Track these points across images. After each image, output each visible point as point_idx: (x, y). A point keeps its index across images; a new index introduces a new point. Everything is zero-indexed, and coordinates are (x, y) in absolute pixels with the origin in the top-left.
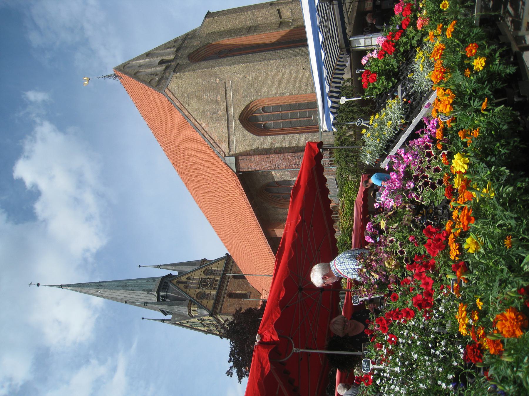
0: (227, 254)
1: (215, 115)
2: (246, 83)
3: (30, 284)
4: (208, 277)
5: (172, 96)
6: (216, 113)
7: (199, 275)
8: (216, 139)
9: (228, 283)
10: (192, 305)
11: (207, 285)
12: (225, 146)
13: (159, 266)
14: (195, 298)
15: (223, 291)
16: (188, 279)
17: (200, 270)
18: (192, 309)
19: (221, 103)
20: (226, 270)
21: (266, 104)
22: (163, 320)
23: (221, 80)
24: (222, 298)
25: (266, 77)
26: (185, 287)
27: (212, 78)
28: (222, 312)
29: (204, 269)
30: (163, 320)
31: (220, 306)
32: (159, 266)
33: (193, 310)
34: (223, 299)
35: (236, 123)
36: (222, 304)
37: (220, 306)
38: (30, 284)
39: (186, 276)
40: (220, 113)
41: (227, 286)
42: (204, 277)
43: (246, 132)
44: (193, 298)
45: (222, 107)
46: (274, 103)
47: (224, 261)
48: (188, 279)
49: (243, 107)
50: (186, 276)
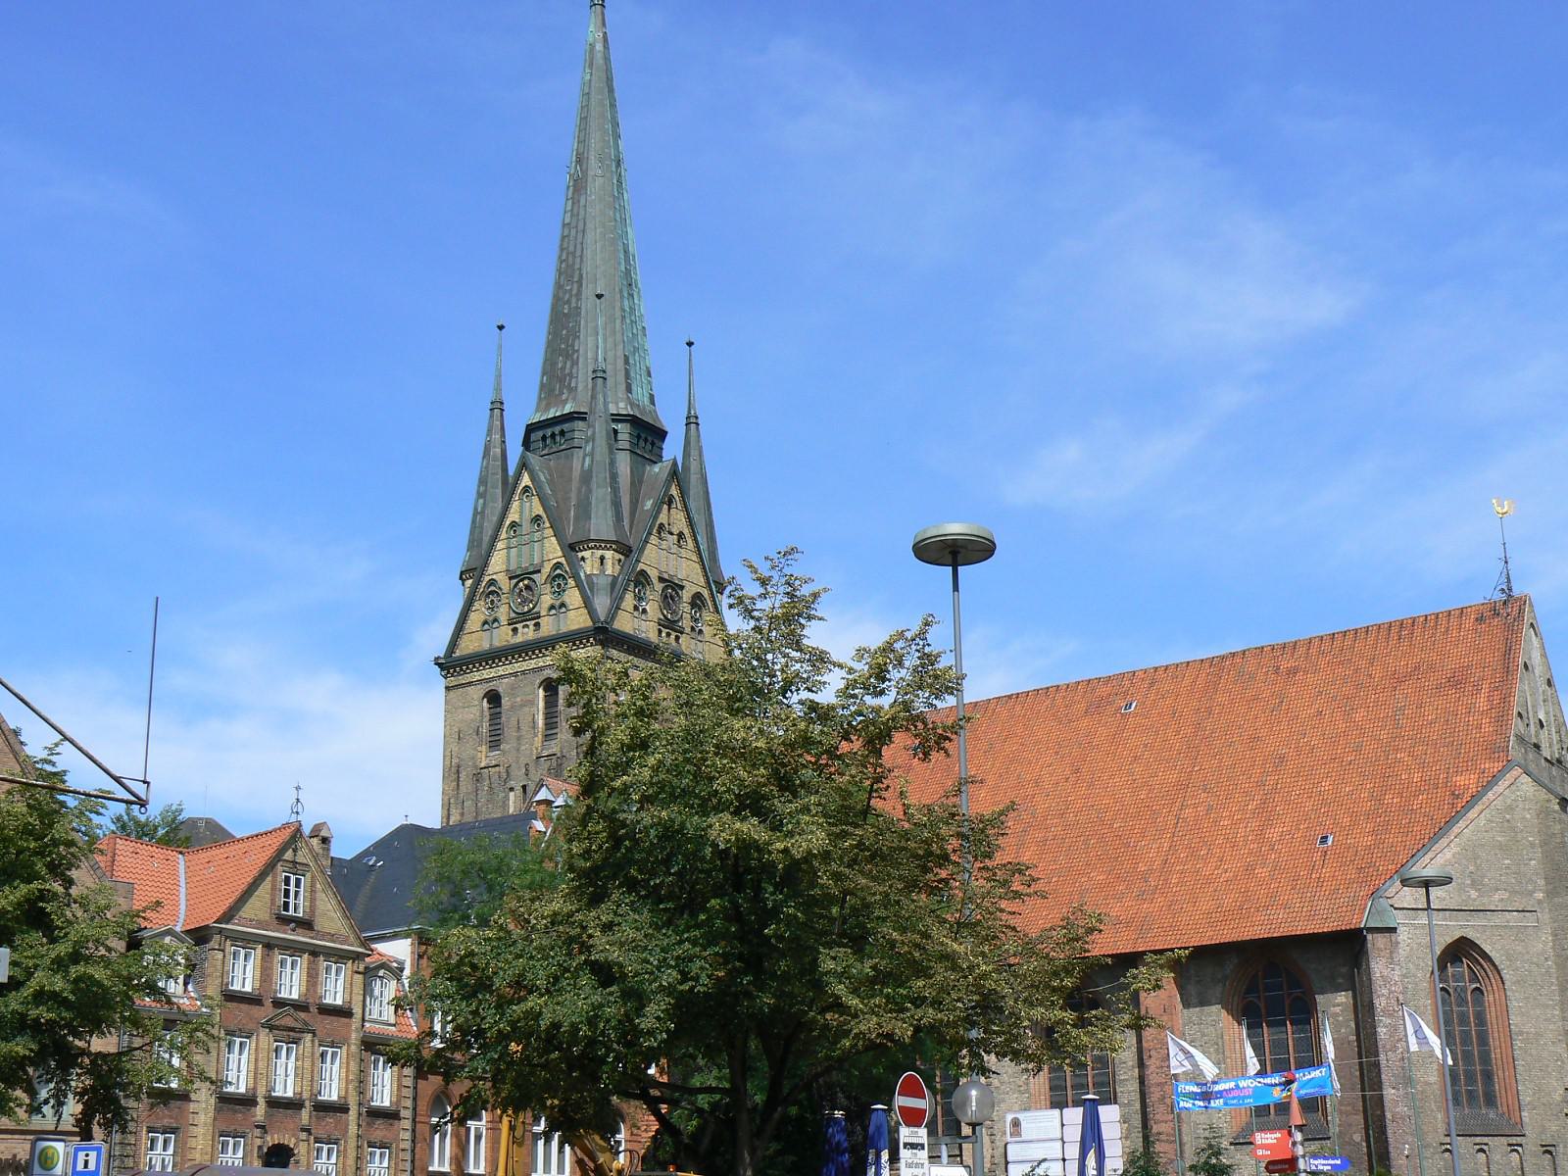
1: (1469, 882)
2: (1535, 960)
4: (687, 608)
5: (1507, 783)
6: (1473, 884)
10: (618, 556)
11: (668, 606)
13: (692, 421)
16: (681, 535)
18: (609, 554)
19: (1496, 900)
21: (1489, 998)
22: (498, 406)
23: (1540, 902)
25: (1548, 1006)
27: (1543, 882)
29: (706, 593)
30: (498, 406)
32: (692, 421)
33: (602, 558)
39: (686, 531)
40: (1474, 894)
42: (686, 595)
44: (638, 561)
45: (1485, 900)
46: (1491, 1015)
49: (1487, 948)
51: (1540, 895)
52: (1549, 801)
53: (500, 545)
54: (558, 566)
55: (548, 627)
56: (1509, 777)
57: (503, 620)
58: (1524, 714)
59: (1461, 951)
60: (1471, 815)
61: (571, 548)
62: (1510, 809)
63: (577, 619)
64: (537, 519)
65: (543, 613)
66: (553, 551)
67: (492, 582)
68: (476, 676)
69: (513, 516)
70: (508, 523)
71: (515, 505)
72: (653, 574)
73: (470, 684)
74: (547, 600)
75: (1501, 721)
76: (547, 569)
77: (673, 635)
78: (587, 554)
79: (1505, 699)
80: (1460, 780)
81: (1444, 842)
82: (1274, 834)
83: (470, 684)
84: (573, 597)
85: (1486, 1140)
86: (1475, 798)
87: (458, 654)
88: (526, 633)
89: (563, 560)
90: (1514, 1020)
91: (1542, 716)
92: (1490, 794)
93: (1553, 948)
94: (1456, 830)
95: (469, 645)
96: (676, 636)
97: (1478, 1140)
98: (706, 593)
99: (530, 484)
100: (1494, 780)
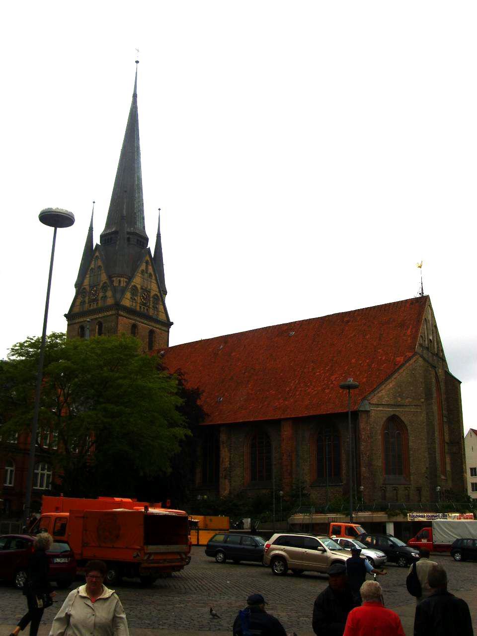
0: (172, 324)
3: (138, 51)
5: (414, 360)
7: (154, 287)
8: (380, 395)
9: (145, 324)
12: (375, 401)
14: (133, 284)
15: (138, 319)
17: (157, 290)
18: (122, 279)
20: (157, 321)
23: (422, 402)
24: (132, 317)
26: (143, 271)
28: (119, 317)
29: (159, 294)
31: (125, 314)
34: (131, 319)
35: (391, 411)
36: (126, 317)
37: (125, 314)
38: (138, 51)
39: (152, 273)
40: (399, 399)
41: (142, 323)
43: (384, 419)
47: (165, 319)
48: (150, 275)
50: (152, 273)
51: (423, 400)
52: (428, 367)
53: (88, 276)
54: (105, 283)
55: (100, 304)
56: (415, 358)
57: (87, 301)
58: (424, 337)
59: (394, 420)
60: (401, 371)
61: (110, 277)
62: (414, 369)
63: (110, 301)
64: (100, 267)
65: (100, 299)
66: (104, 277)
67: (84, 289)
68: (77, 321)
69: (92, 266)
70: (90, 268)
71: (93, 262)
72: (139, 287)
73: (75, 323)
74: (101, 295)
75: (415, 338)
76: (101, 285)
77: (146, 308)
78: (114, 279)
79: (417, 331)
80: (398, 359)
81: (390, 381)
82: (333, 378)
83: (75, 323)
84: (109, 294)
85: (397, 486)
86: (403, 365)
87: (72, 313)
88: (94, 306)
89: (107, 281)
90: (411, 444)
91: (431, 338)
92: (408, 364)
93: (426, 419)
94: (394, 376)
95: (76, 310)
96: (147, 309)
97: (394, 486)
98: (159, 294)
99: (144, 269)
100: (410, 359)
